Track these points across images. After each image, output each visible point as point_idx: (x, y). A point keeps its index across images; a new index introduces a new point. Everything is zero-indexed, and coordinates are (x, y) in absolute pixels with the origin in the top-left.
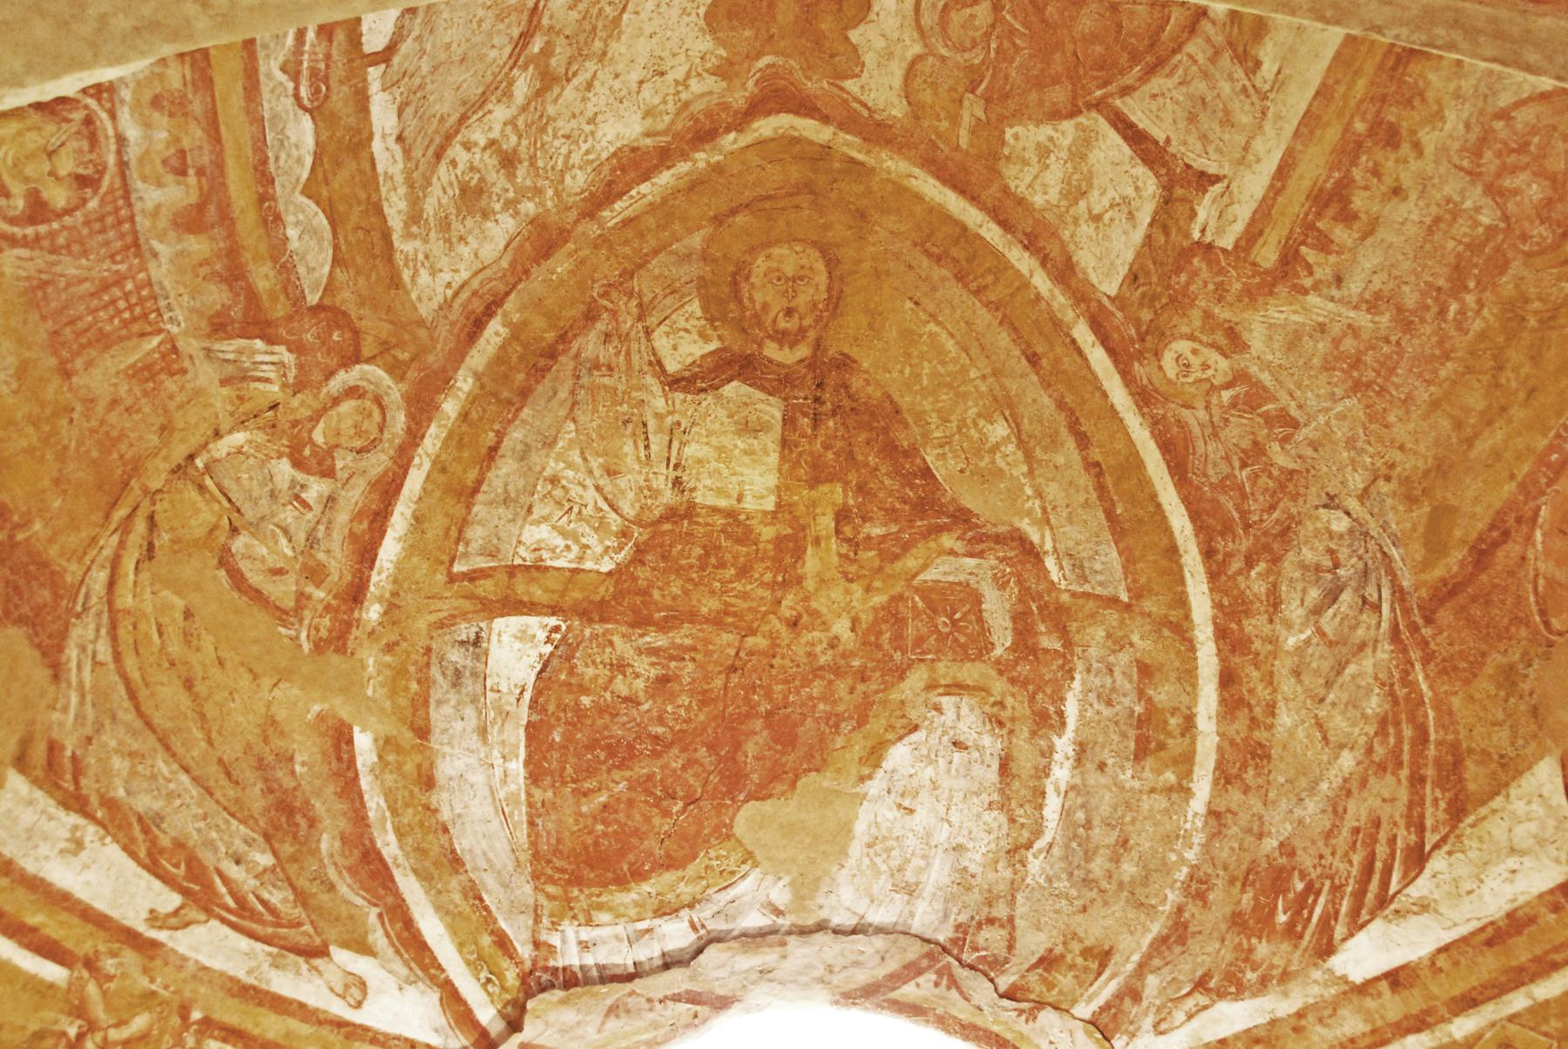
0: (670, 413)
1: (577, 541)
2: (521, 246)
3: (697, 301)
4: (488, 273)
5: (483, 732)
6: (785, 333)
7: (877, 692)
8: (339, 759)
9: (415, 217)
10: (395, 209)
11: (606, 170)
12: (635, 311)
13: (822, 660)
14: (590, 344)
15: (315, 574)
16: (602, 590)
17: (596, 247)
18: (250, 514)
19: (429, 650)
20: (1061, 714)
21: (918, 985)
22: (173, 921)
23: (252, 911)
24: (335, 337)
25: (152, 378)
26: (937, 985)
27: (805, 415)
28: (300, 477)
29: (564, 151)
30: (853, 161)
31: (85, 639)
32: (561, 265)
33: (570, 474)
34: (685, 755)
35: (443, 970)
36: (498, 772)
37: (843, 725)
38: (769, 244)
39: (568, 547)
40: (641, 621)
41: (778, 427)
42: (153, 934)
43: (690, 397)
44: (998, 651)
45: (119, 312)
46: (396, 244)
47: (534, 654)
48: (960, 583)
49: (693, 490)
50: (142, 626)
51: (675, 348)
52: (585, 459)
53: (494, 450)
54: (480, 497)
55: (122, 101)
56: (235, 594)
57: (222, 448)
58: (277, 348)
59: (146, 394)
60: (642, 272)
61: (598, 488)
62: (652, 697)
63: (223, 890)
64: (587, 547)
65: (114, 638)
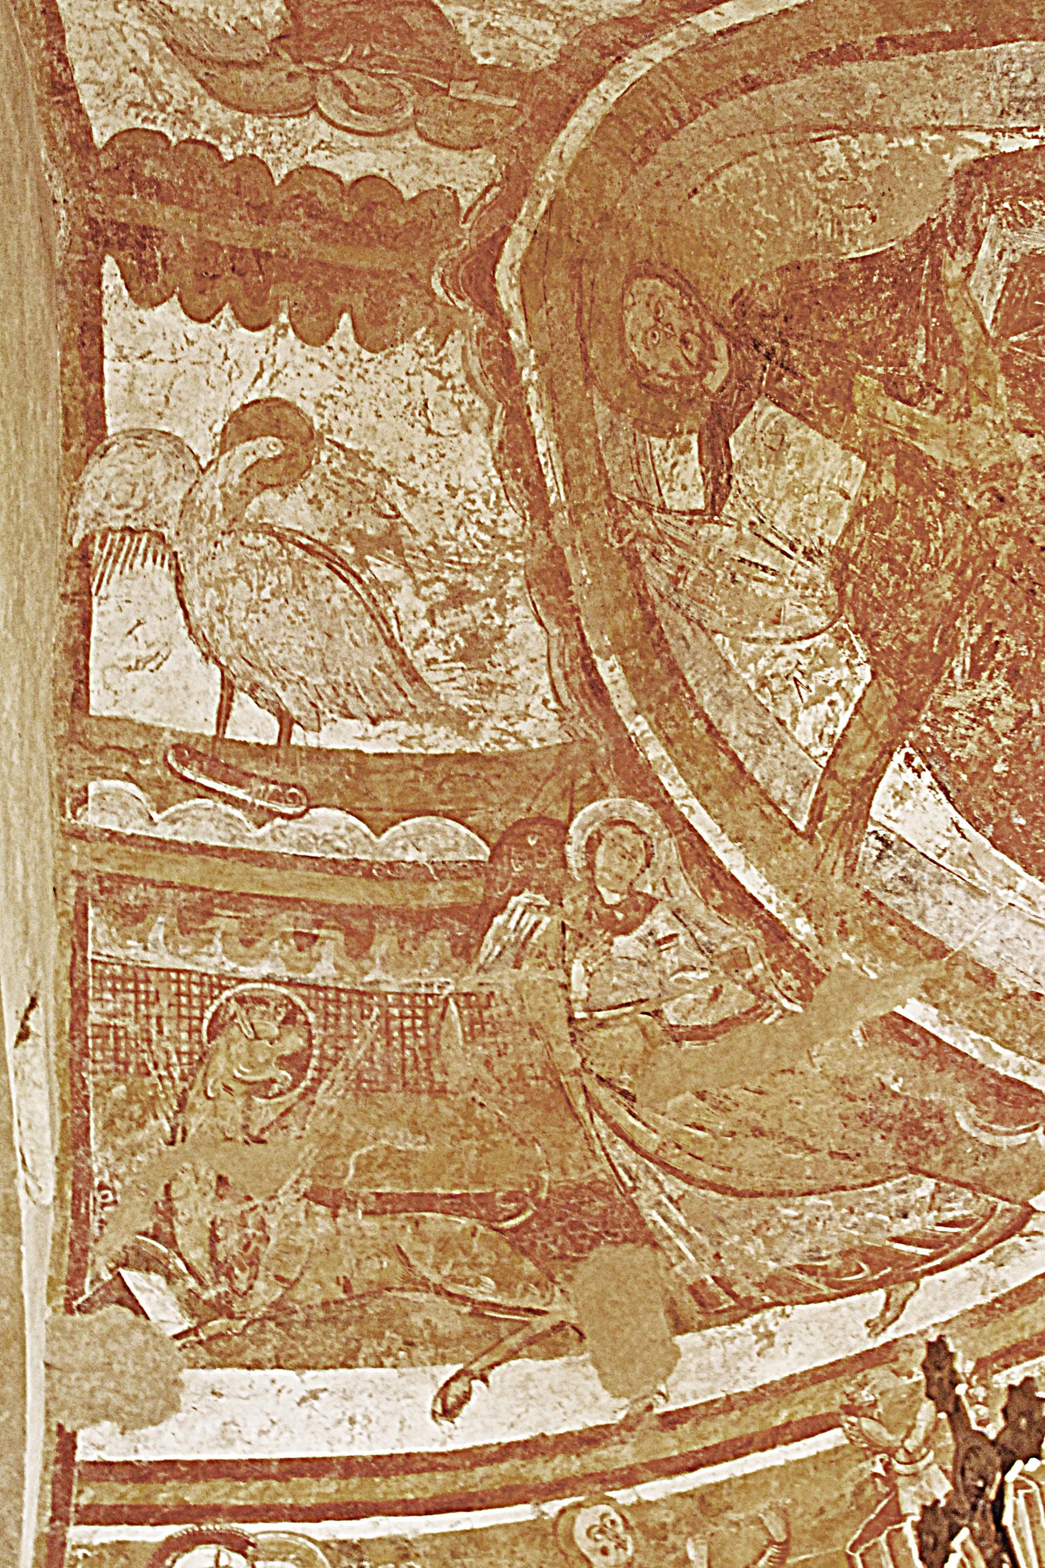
0: (739, 529)
1: (829, 691)
2: (547, 606)
4: (554, 653)
5: (974, 891)
8: (915, 1043)
9: (460, 721)
10: (443, 741)
11: (512, 484)
14: (656, 577)
15: (738, 960)
16: (887, 691)
18: (651, 993)
19: (867, 894)
22: (889, 1315)
23: (948, 1240)
24: (532, 843)
25: (483, 1024)
28: (641, 931)
29: (473, 529)
31: (655, 1198)
32: (580, 570)
33: (762, 662)
36: (1020, 902)
39: (832, 703)
40: (937, 669)
42: (883, 1339)
45: (413, 1028)
46: (476, 749)
47: (925, 792)
48: (1010, 276)
50: (683, 1140)
52: (755, 640)
55: (234, 971)
56: (711, 1043)
57: (579, 988)
58: (511, 905)
59: (494, 1034)
61: (786, 642)
62: (1029, 696)
63: (912, 1249)
64: (839, 682)
65: (674, 1171)
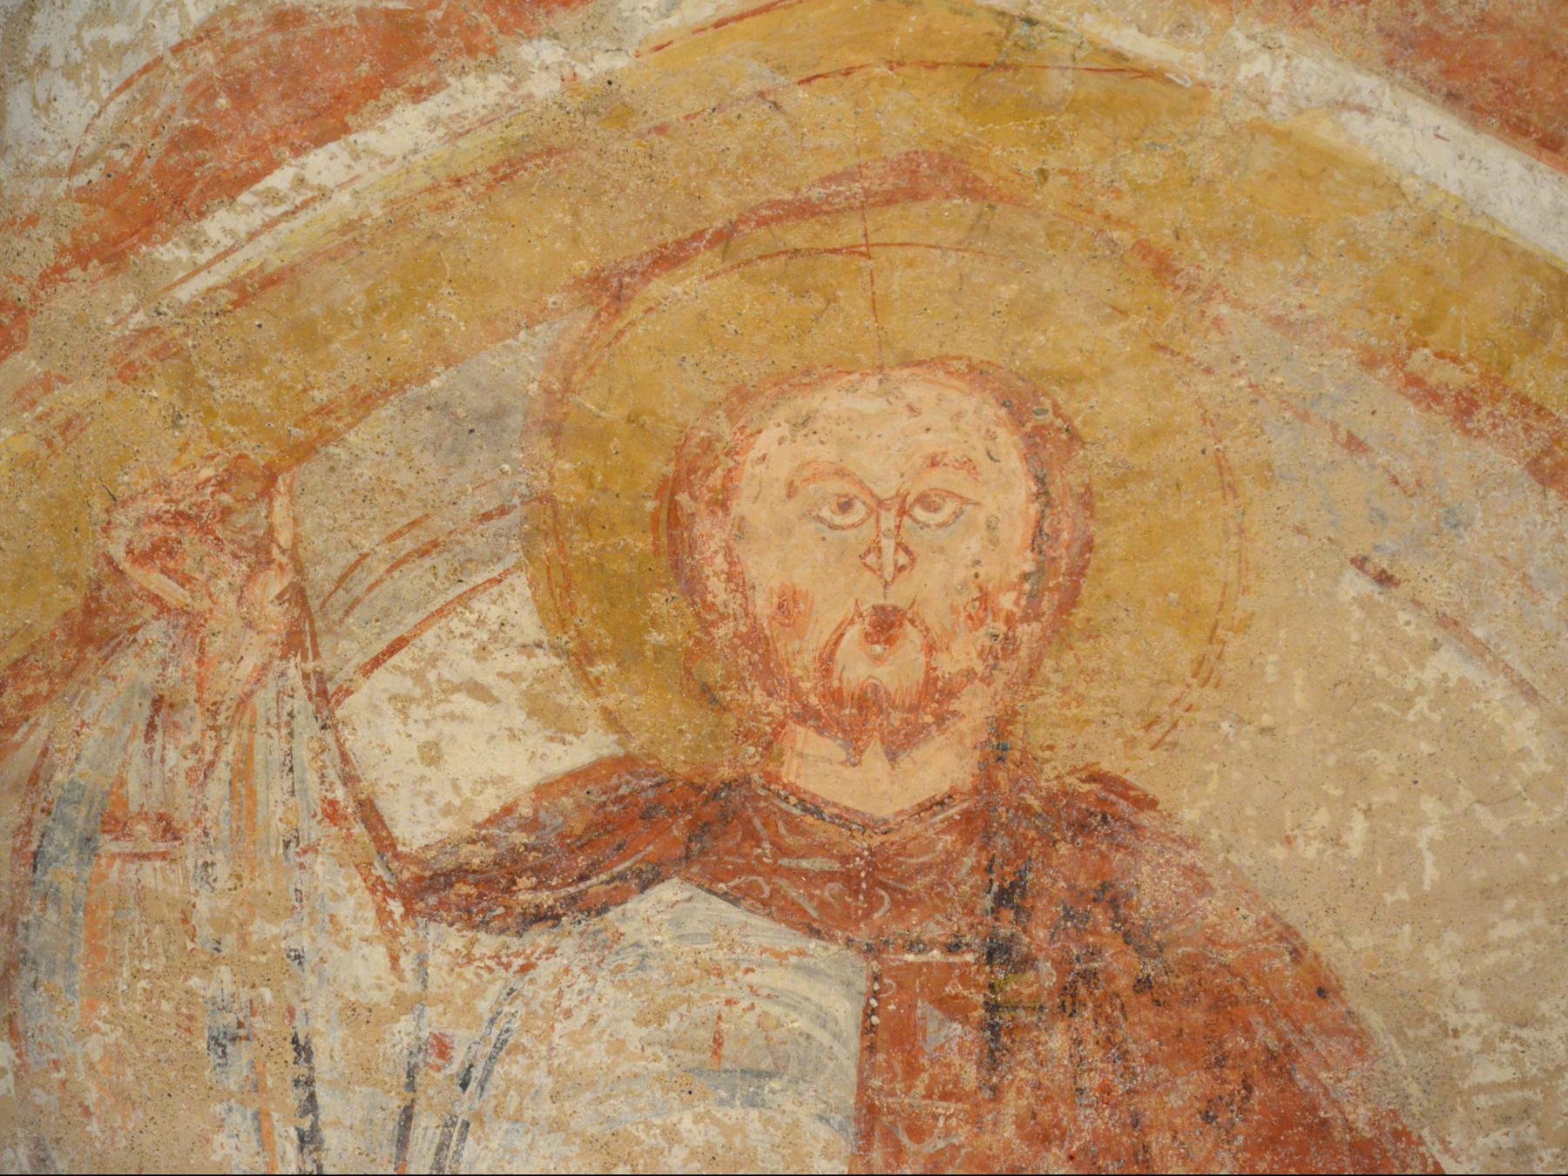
0: (403, 1004)
3: (520, 581)
6: (868, 701)
12: (276, 617)
17: (129, 373)
27: (953, 1009)
30: (1120, 65)
38: (806, 377)
41: (847, 1053)
43: (487, 943)
51: (431, 754)
60: (312, 473)
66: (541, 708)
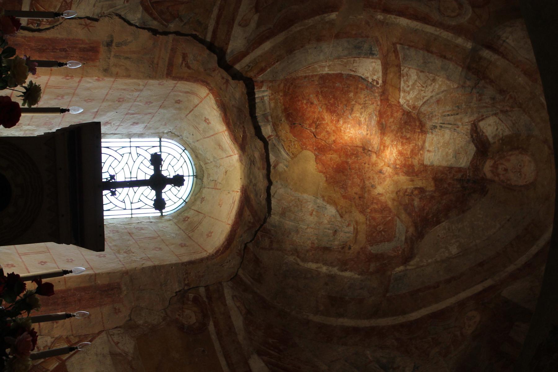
0: (462, 124)
1: (411, 90)
3: (510, 133)
6: (497, 168)
7: (355, 202)
13: (367, 182)
14: (490, 91)
16: (393, 100)
19: (368, 37)
20: (346, 270)
21: (249, 216)
26: (250, 222)
27: (462, 176)
33: (437, 86)
34: (332, 131)
35: (252, 51)
37: (343, 190)
39: (408, 86)
41: (458, 166)
43: (469, 131)
44: (369, 248)
47: (368, 75)
48: (395, 234)
49: (432, 133)
51: (489, 125)
52: (443, 92)
53: (445, 57)
54: (426, 53)
61: (432, 97)
64: (409, 93)
66: (496, 135)
